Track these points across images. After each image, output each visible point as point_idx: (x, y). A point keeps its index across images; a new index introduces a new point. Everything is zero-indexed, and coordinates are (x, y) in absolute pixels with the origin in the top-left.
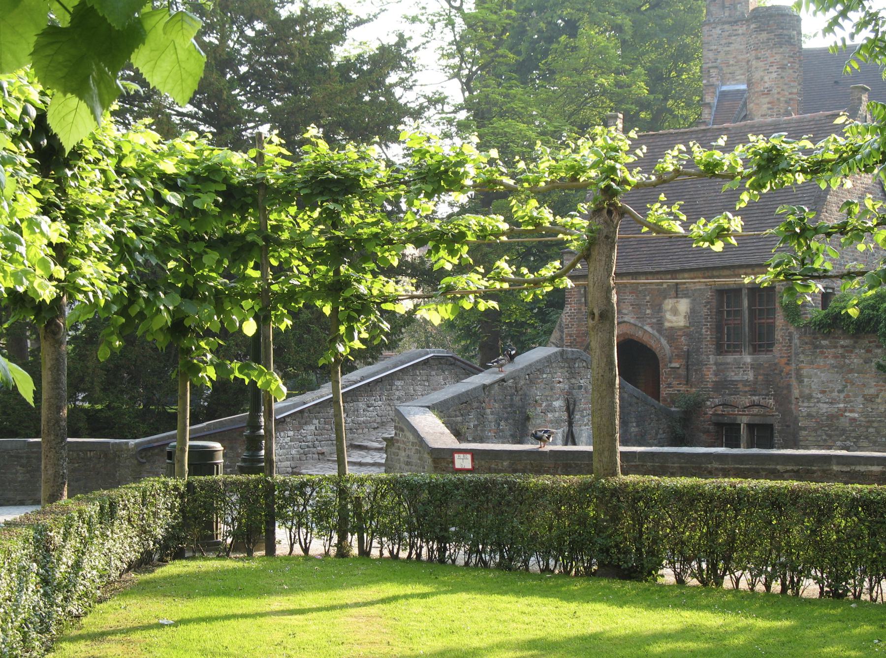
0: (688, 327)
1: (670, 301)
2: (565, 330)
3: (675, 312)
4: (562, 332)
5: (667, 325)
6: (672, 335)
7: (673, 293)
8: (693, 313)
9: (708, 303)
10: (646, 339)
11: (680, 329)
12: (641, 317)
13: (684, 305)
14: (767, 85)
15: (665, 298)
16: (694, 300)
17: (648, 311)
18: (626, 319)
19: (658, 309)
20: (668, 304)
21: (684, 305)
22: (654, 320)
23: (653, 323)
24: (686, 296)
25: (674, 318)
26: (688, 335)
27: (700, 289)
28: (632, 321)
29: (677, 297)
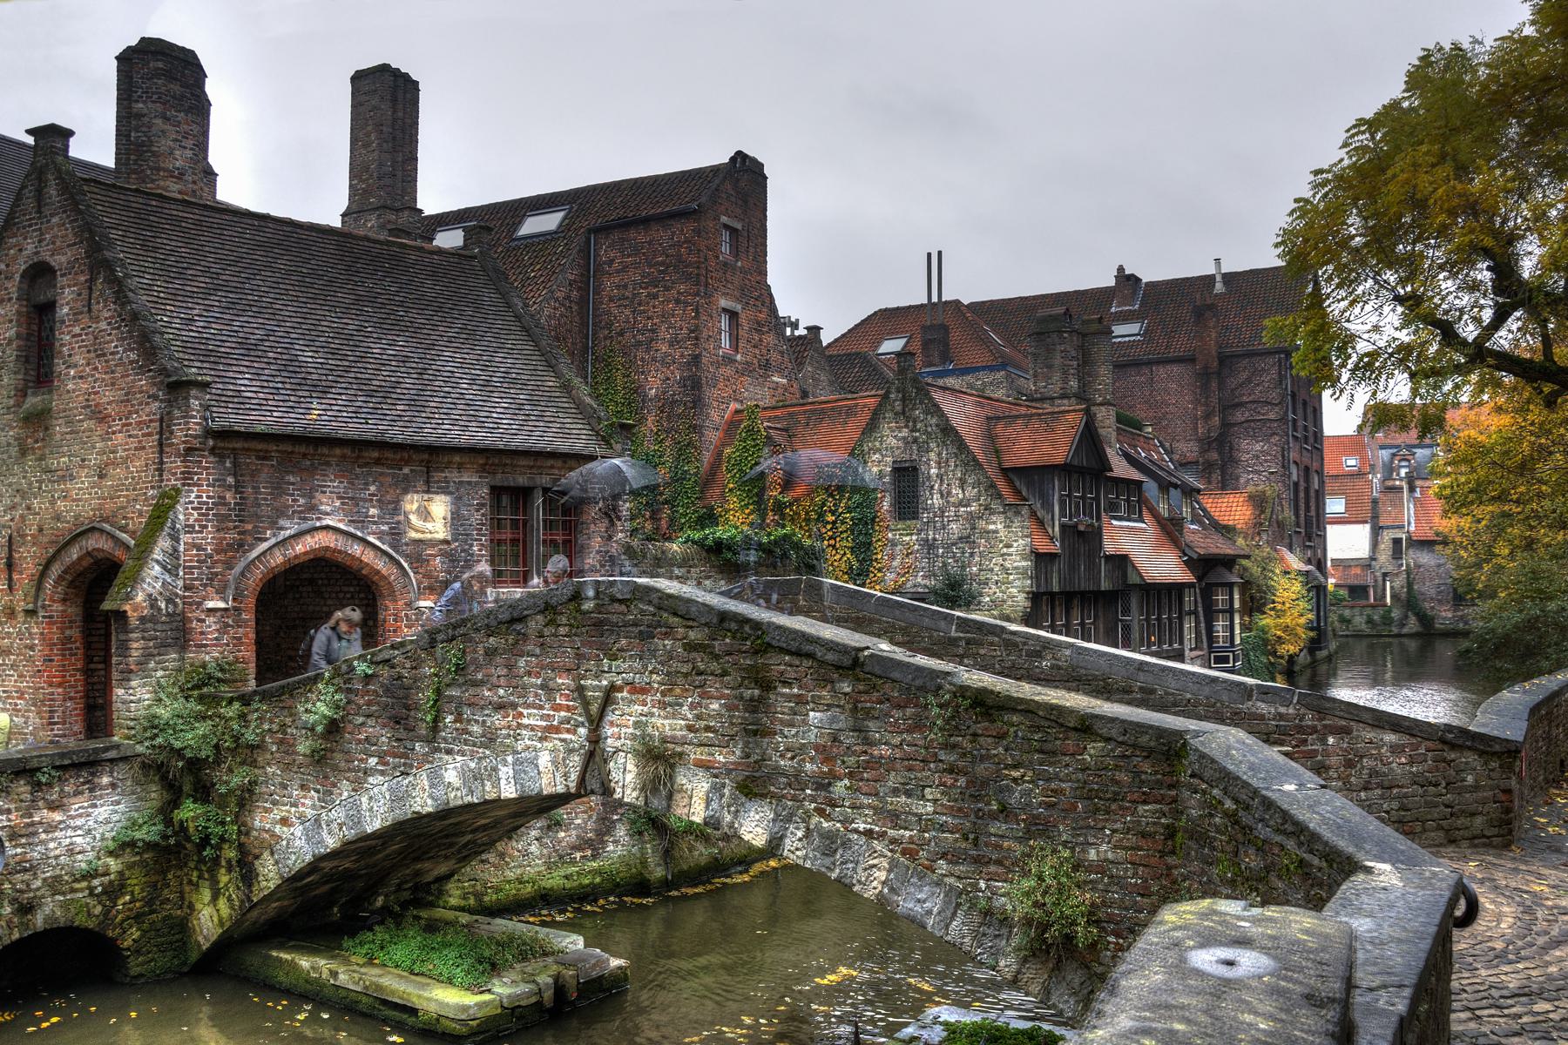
0: (446, 542)
1: (416, 497)
2: (185, 538)
3: (426, 515)
4: (177, 540)
5: (413, 535)
6: (418, 552)
7: (420, 485)
8: (456, 519)
9: (483, 505)
10: (369, 557)
11: (432, 543)
12: (361, 522)
13: (440, 507)
14: (178, 164)
15: (406, 491)
16: (459, 498)
17: (373, 511)
18: (331, 523)
19: (396, 510)
20: (411, 503)
21: (440, 507)
22: (385, 528)
23: (382, 532)
24: (445, 491)
25: (429, 526)
26: (451, 557)
27: (469, 483)
28: (341, 526)
29: (428, 492)
